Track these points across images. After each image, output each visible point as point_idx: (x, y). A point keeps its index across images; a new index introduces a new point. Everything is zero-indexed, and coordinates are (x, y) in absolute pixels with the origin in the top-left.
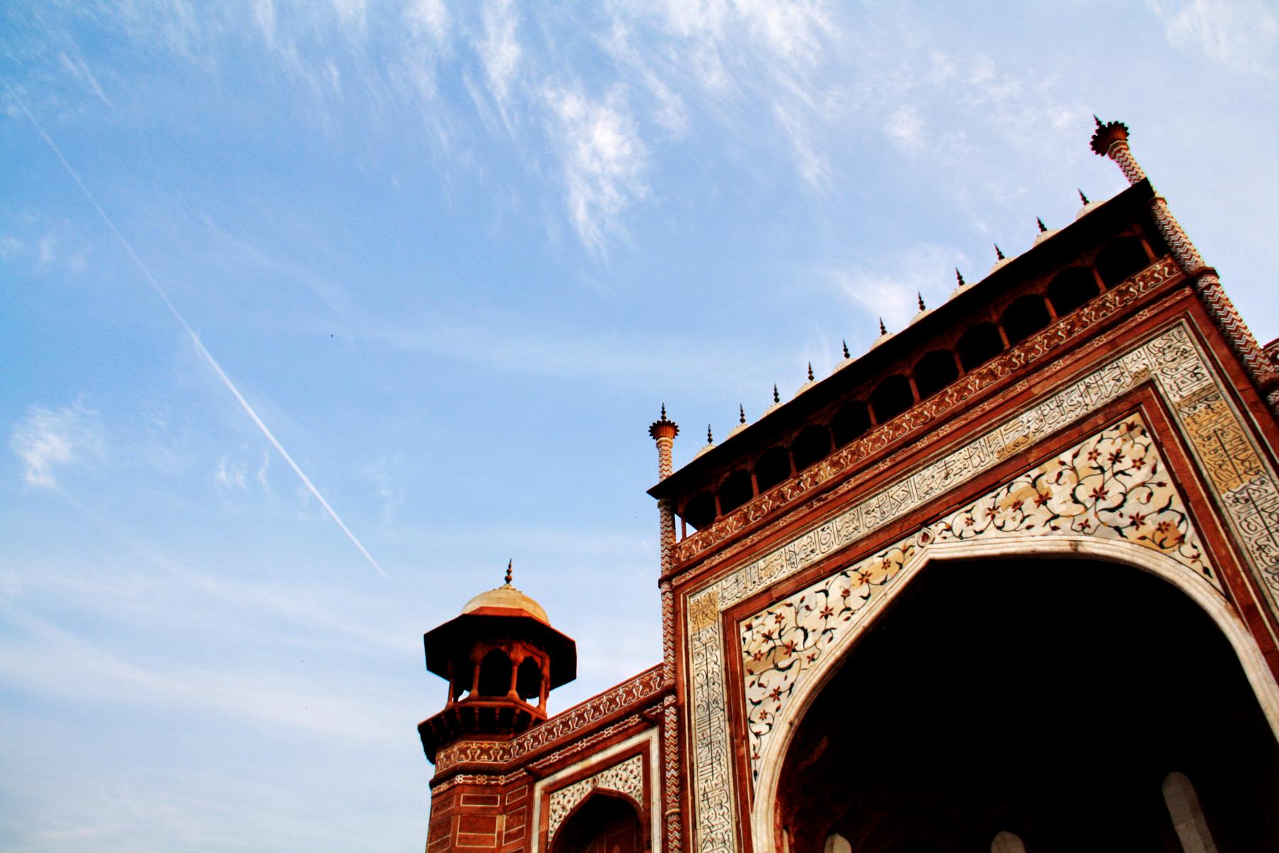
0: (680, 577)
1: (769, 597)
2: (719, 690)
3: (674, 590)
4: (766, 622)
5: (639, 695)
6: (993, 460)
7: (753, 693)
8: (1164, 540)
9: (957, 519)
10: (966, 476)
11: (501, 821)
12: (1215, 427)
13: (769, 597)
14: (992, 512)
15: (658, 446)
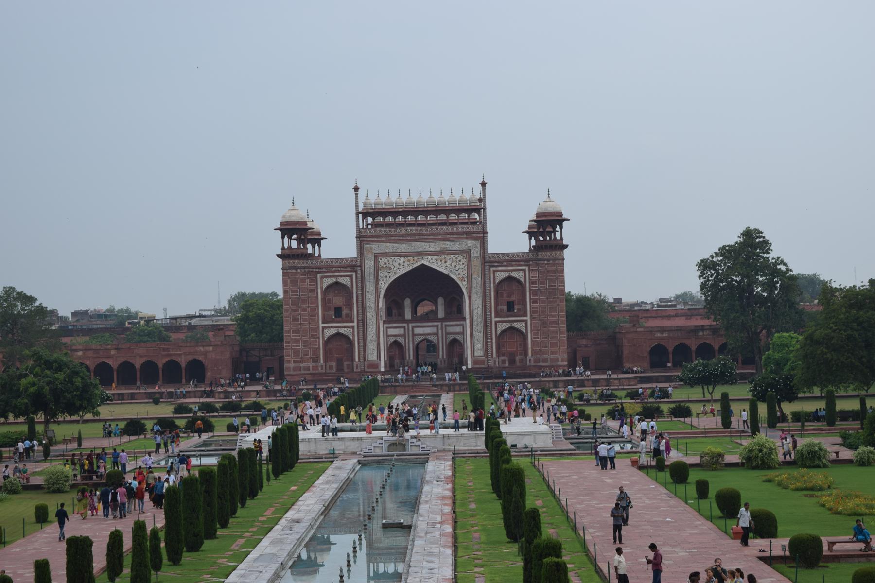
0: (362, 238)
1: (386, 255)
2: (372, 270)
3: (361, 242)
4: (385, 260)
5: (349, 263)
6: (439, 249)
7: (381, 275)
8: (462, 280)
9: (429, 258)
10: (432, 249)
11: (308, 280)
12: (477, 264)
13: (386, 255)
14: (436, 260)
15: (356, 195)
